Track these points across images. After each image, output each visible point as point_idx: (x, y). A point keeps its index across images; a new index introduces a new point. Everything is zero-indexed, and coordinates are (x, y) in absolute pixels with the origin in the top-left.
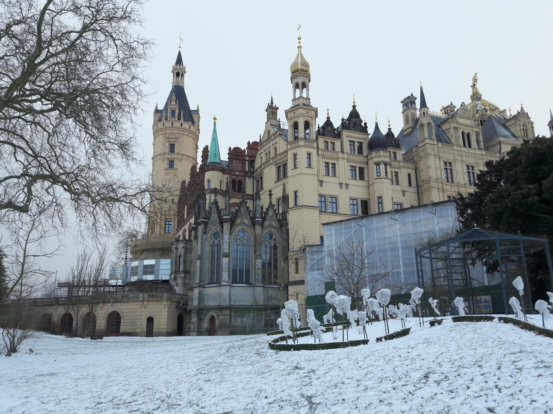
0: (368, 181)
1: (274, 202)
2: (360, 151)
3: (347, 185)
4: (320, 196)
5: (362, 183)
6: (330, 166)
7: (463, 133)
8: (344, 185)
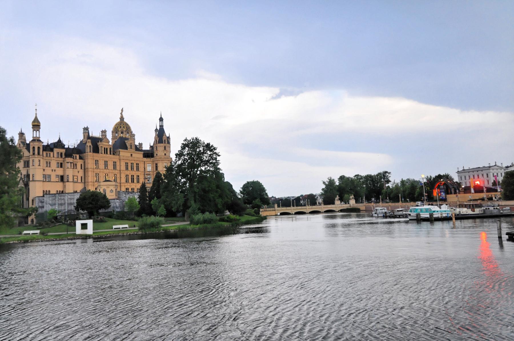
0: (64, 168)
1: (23, 177)
2: (61, 156)
3: (55, 170)
4: (43, 175)
5: (62, 169)
6: (48, 163)
7: (105, 148)
8: (54, 170)
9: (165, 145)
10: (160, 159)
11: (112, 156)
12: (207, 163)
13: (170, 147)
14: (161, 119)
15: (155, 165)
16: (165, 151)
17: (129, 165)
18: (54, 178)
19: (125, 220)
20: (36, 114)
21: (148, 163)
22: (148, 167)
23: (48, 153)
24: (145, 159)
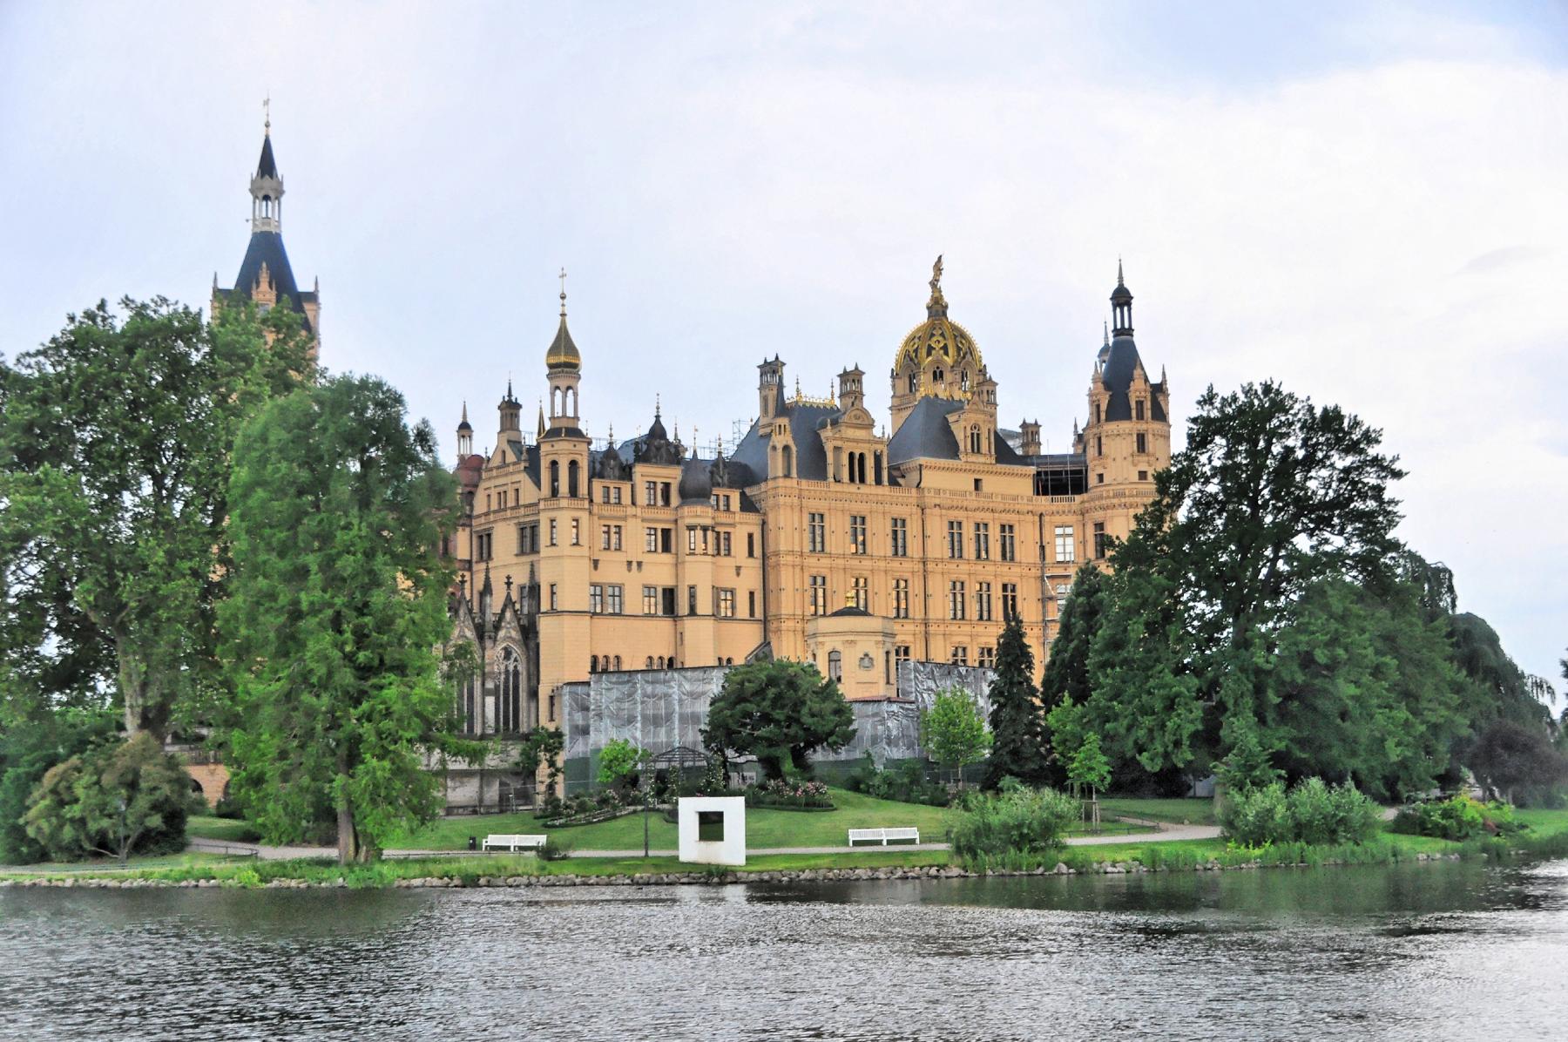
1: (515, 596)
3: (639, 564)
4: (594, 585)
7: (851, 455)
8: (634, 565)
9: (1142, 426)
10: (1115, 501)
11: (885, 490)
12: (1321, 515)
13: (1169, 437)
14: (1122, 298)
15: (1091, 531)
16: (1144, 458)
17: (969, 532)
18: (635, 602)
19: (923, 803)
20: (563, 315)
21: (1058, 519)
22: (1059, 541)
23: (612, 484)
24: (1044, 502)
